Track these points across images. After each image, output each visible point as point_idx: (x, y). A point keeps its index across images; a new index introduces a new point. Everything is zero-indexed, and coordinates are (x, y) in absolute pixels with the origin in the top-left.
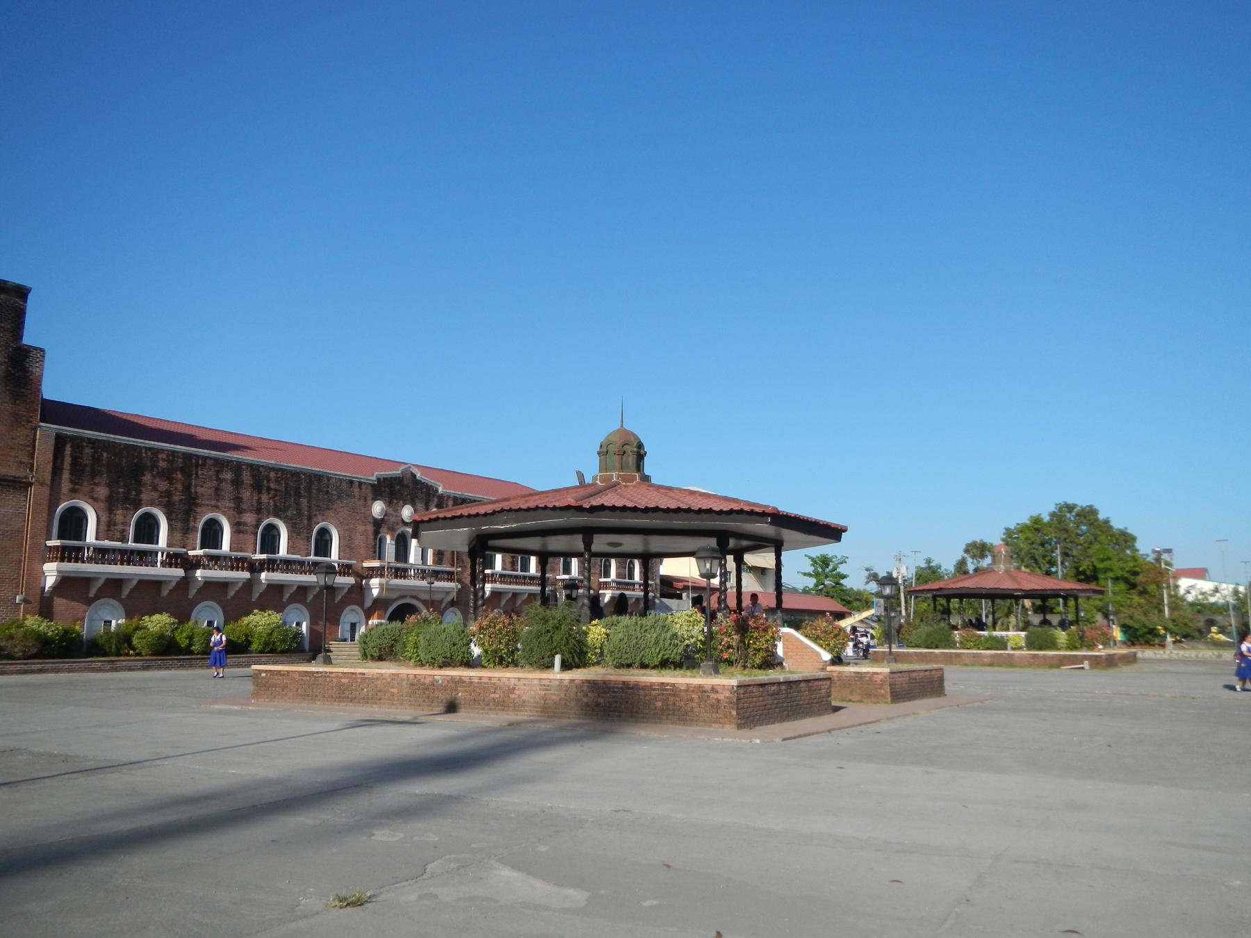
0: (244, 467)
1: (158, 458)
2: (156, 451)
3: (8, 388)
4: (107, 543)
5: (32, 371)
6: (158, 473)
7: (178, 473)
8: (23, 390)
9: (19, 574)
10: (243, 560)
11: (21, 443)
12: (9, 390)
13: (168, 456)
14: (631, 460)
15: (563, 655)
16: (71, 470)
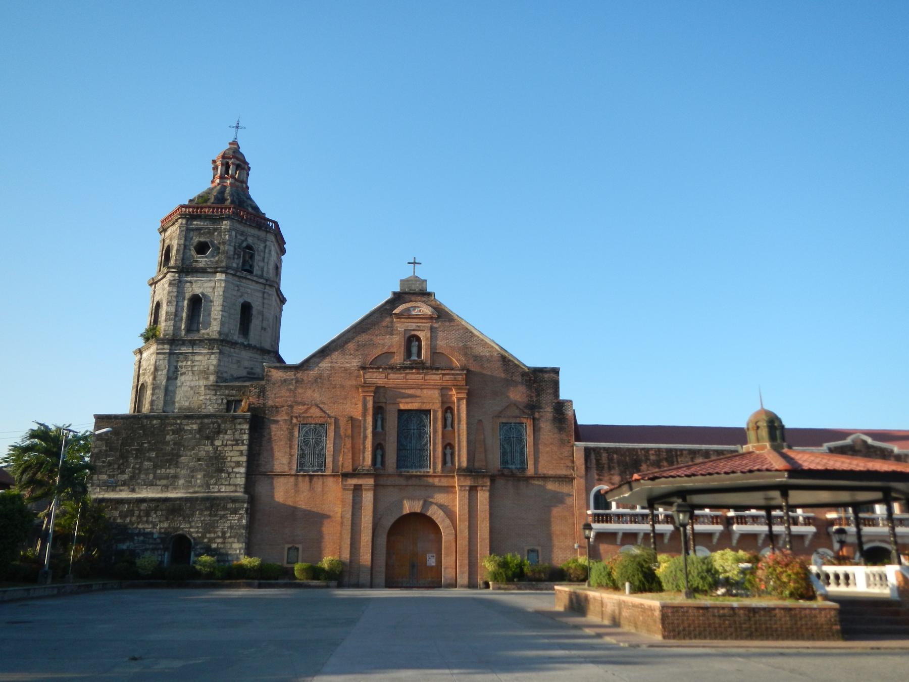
0: (711, 453)
1: (648, 454)
2: (647, 450)
3: (556, 425)
4: (621, 511)
5: (567, 414)
6: (650, 463)
7: (664, 462)
8: (564, 425)
9: (574, 531)
10: (717, 517)
11: (566, 455)
12: (556, 427)
13: (656, 451)
14: (764, 432)
15: (630, 582)
16: (596, 468)
